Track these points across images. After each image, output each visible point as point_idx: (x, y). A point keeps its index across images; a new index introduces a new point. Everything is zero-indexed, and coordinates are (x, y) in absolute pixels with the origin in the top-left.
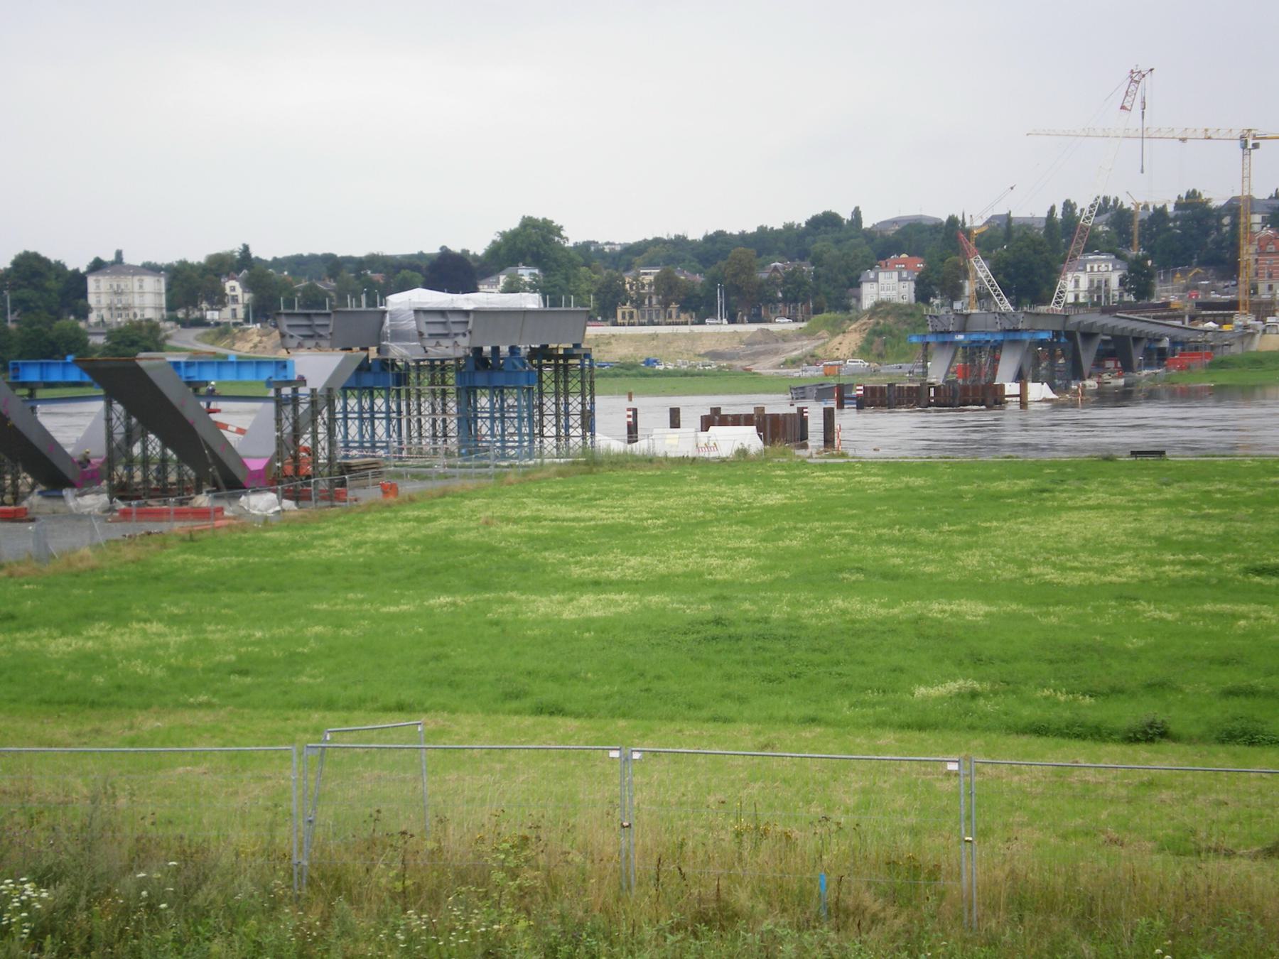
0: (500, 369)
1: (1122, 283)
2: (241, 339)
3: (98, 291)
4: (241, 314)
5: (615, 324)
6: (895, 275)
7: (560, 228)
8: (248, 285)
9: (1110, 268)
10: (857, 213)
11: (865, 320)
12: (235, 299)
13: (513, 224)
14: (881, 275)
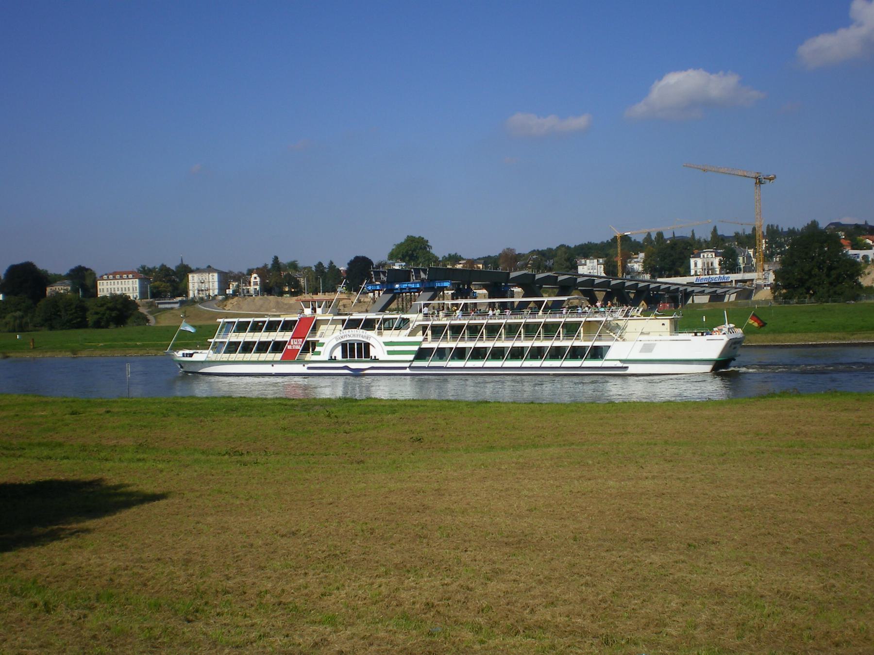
1: (720, 264)
6: (596, 261)
9: (714, 256)
14: (588, 261)
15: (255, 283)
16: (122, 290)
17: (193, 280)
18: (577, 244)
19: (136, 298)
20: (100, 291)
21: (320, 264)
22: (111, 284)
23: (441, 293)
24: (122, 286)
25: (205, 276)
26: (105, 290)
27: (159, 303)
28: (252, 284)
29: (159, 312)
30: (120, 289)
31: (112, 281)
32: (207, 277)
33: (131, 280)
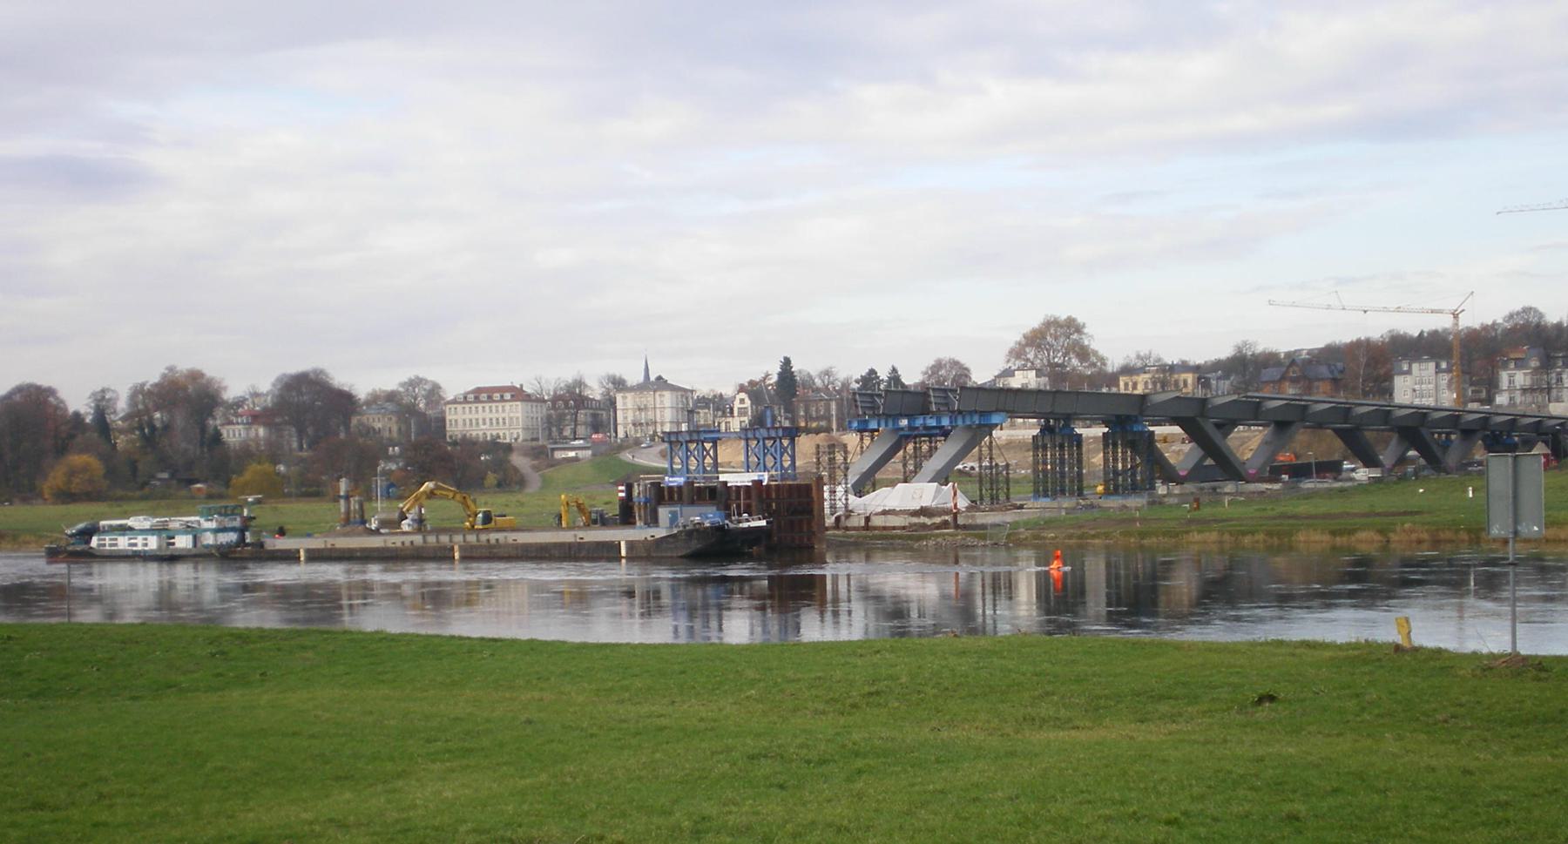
3: (626, 406)
6: (1432, 365)
14: (1415, 366)
15: (742, 412)
16: (465, 424)
17: (625, 404)
18: (1426, 330)
19: (516, 439)
20: (451, 424)
21: (872, 372)
22: (470, 412)
23: (987, 438)
24: (470, 416)
25: (648, 398)
26: (460, 422)
27: (553, 450)
28: (736, 413)
29: (552, 466)
30: (488, 421)
31: (473, 406)
32: (651, 399)
33: (507, 405)
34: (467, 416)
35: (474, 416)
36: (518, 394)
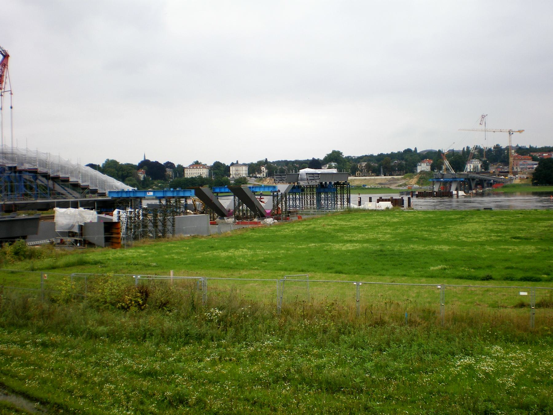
0: (326, 187)
2: (265, 181)
3: (233, 170)
4: (265, 175)
5: (356, 176)
6: (426, 164)
7: (342, 153)
8: (267, 168)
10: (416, 149)
11: (418, 175)
12: (264, 171)
13: (330, 152)
14: (422, 164)
33: (201, 169)
34: (190, 172)
35: (192, 172)
36: (204, 166)
